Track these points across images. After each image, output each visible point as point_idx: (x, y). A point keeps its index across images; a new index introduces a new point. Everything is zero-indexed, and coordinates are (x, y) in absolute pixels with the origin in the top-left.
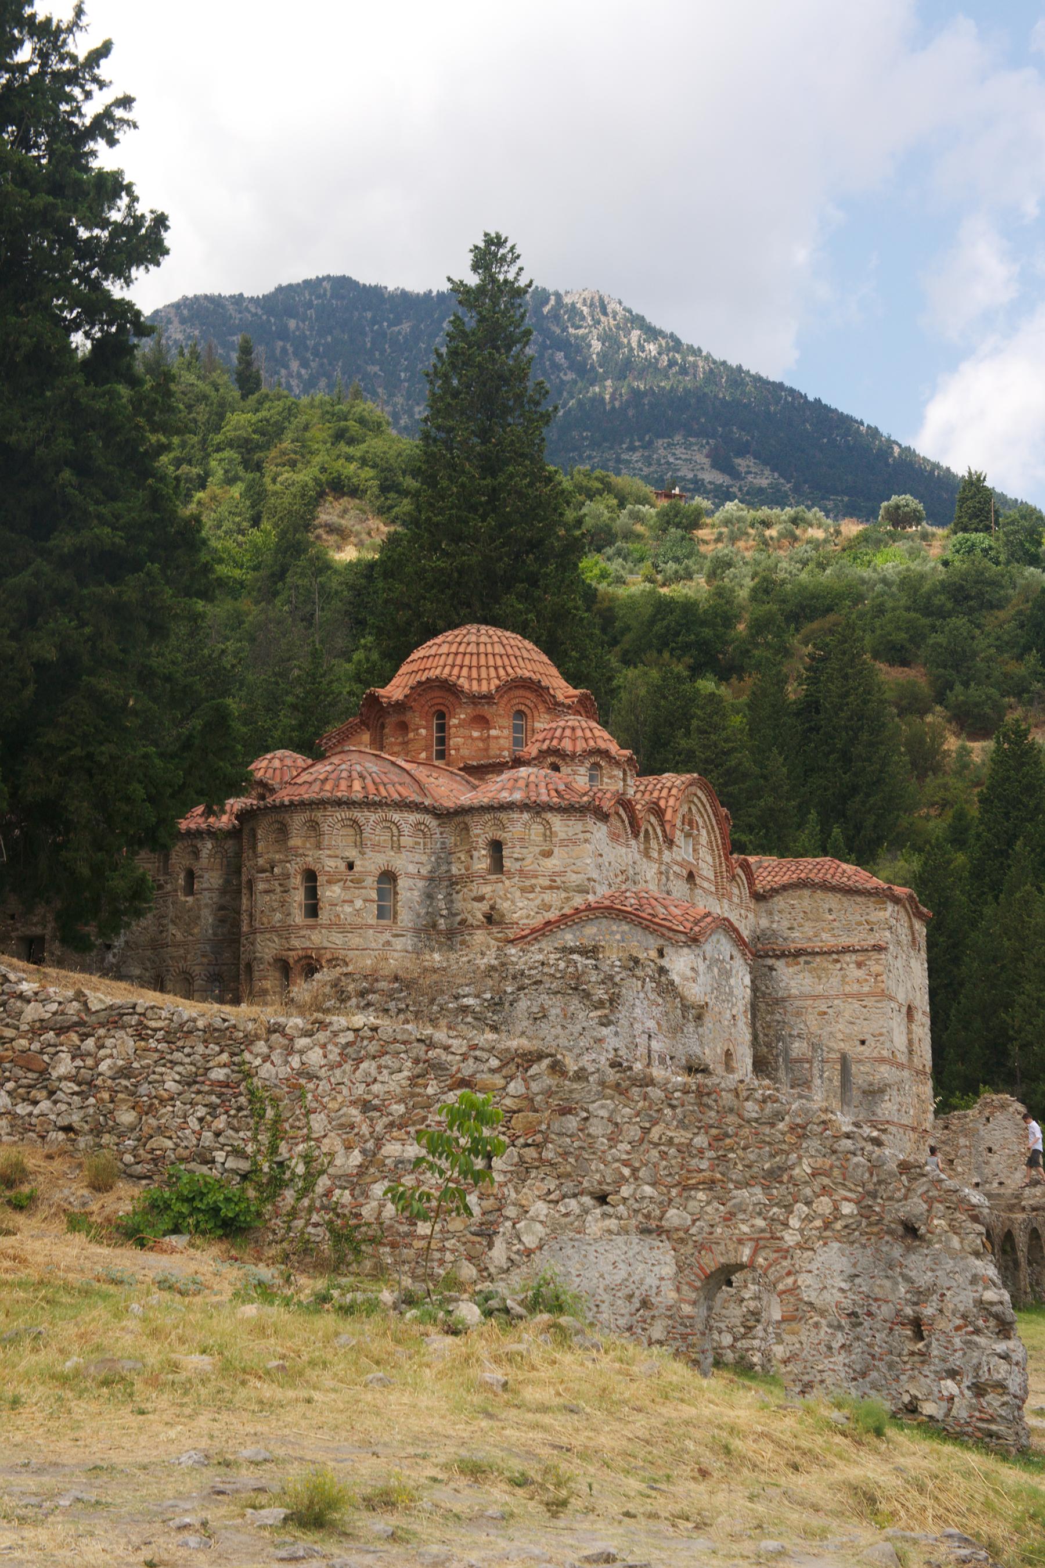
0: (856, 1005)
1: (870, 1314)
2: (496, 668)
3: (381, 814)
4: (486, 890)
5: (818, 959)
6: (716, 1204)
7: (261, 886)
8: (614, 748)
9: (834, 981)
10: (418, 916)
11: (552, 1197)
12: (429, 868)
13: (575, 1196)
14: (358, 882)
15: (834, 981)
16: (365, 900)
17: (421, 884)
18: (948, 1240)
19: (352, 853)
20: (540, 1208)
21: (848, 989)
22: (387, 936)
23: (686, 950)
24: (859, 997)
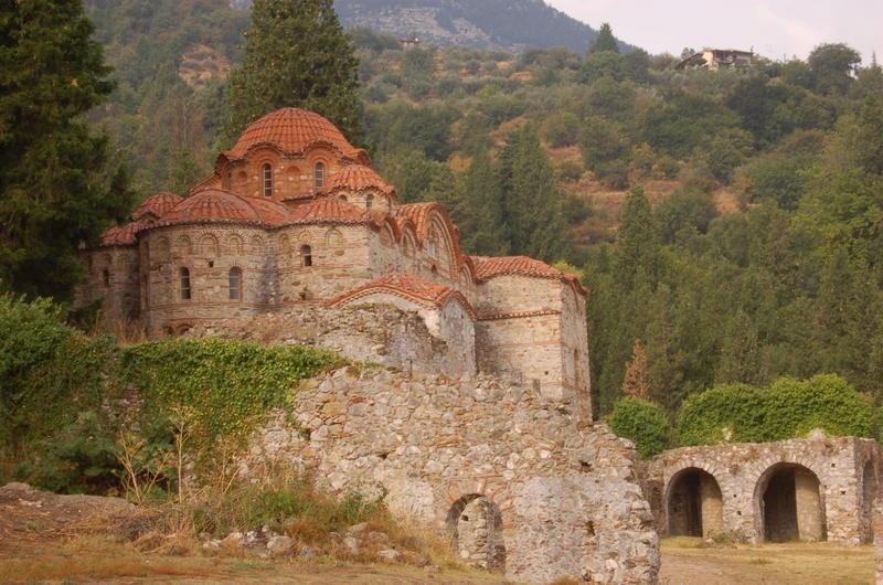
0: (542, 349)
1: (560, 521)
2: (303, 135)
4: (301, 277)
5: (517, 320)
6: (459, 456)
7: (152, 279)
8: (381, 185)
9: (528, 335)
10: (257, 296)
11: (351, 456)
12: (262, 264)
13: (366, 455)
15: (528, 335)
16: (222, 287)
17: (257, 275)
18: (610, 471)
19: (211, 256)
20: (345, 464)
21: (536, 339)
22: (236, 310)
24: (544, 344)
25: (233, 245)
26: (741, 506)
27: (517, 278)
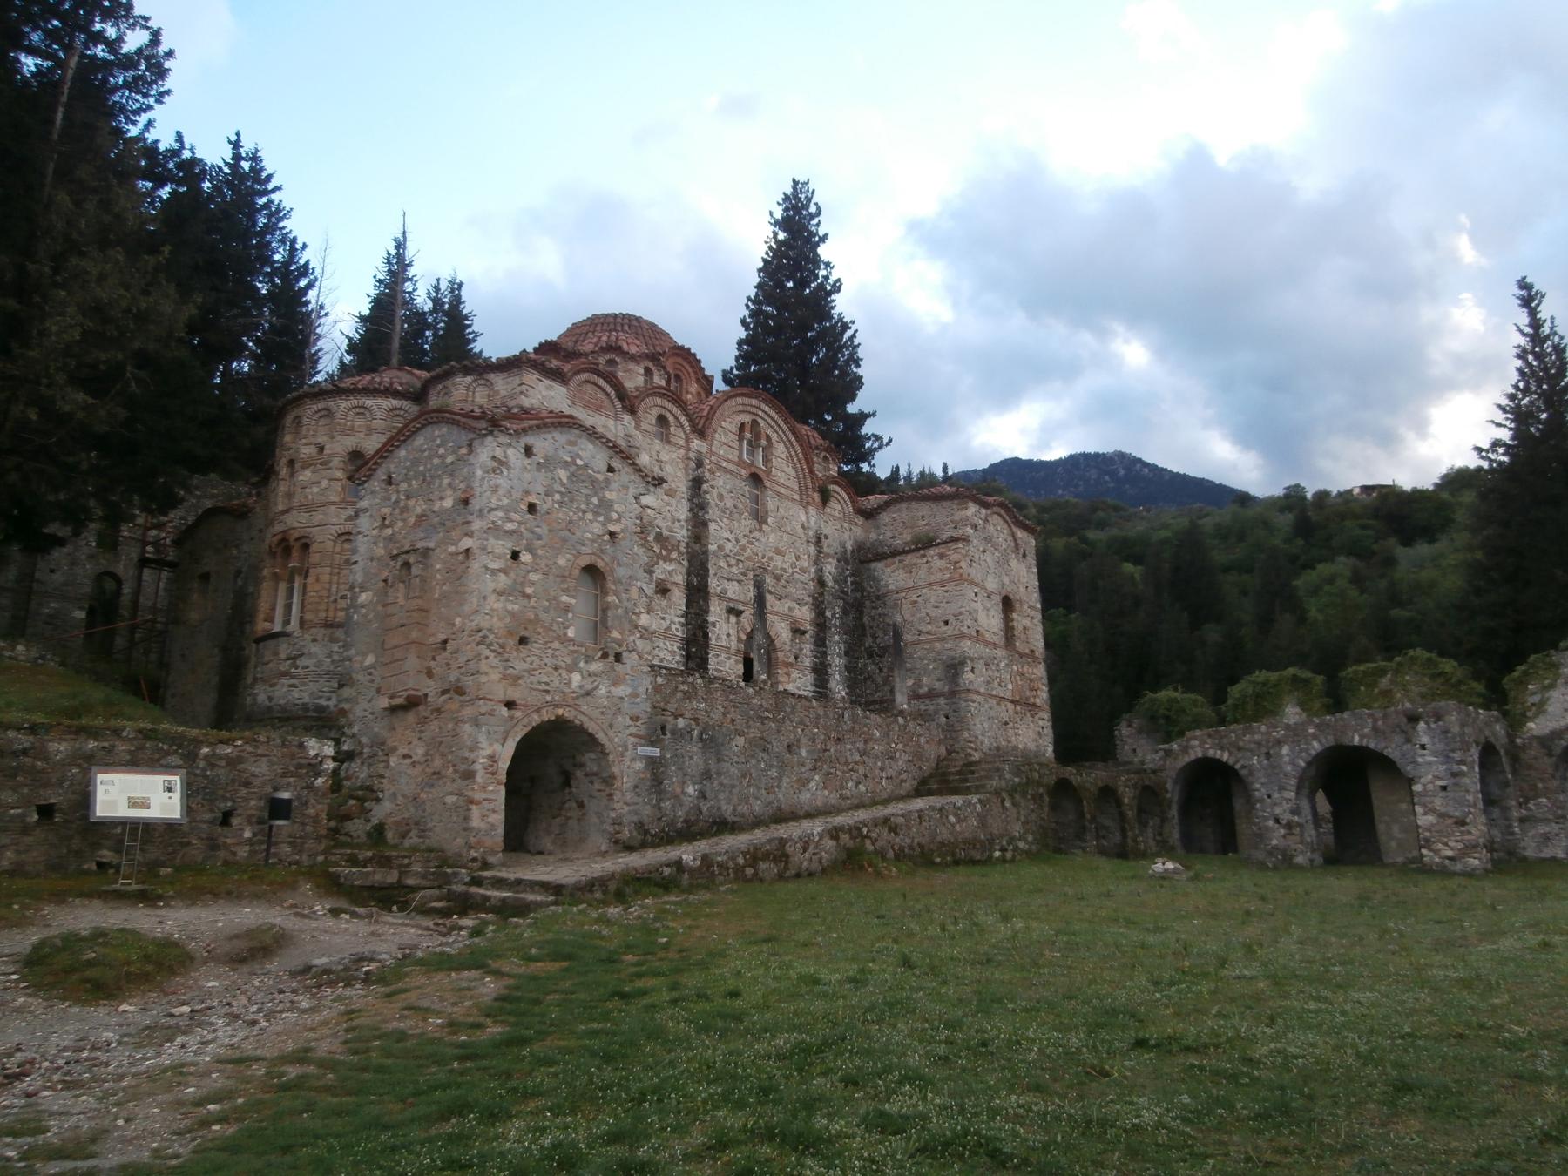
0: (940, 591)
3: (353, 401)
14: (326, 464)
15: (922, 574)
19: (322, 439)
21: (933, 578)
23: (490, 438)
24: (941, 583)
25: (359, 423)
26: (1277, 811)
27: (914, 505)
